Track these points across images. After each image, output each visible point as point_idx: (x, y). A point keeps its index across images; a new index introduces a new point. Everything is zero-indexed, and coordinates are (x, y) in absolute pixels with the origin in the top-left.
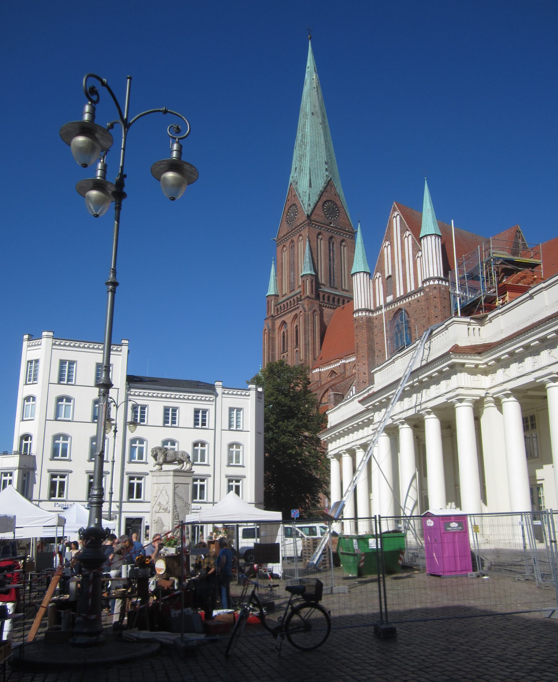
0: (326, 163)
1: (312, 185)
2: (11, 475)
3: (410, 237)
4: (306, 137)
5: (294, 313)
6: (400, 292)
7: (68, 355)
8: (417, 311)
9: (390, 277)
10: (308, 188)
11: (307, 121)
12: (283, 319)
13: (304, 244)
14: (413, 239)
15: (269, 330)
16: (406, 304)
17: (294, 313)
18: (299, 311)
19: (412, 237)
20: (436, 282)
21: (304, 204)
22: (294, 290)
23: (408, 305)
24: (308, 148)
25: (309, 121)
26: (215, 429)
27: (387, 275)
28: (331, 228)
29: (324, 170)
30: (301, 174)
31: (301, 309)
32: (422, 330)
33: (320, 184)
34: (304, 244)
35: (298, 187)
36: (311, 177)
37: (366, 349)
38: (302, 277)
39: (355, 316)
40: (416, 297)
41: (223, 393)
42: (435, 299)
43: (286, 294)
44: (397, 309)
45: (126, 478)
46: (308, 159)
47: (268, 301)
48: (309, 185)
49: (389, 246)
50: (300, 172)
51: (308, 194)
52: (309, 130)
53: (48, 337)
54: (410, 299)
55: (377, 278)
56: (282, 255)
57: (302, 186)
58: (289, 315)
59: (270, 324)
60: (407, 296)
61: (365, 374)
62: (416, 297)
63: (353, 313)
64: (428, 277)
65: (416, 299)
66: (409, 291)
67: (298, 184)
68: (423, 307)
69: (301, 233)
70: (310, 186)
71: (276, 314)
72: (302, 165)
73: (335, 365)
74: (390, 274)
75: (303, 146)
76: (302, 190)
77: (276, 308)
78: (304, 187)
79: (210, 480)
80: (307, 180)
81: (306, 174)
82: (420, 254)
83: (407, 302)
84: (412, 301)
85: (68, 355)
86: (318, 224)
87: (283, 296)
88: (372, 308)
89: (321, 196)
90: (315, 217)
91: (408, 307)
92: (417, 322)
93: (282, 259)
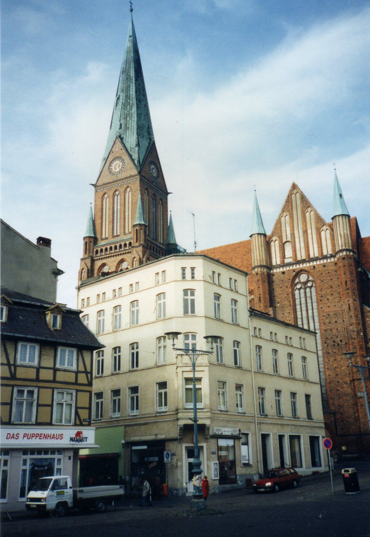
4: (131, 99)
5: (120, 258)
8: (324, 274)
11: (131, 84)
12: (104, 261)
15: (88, 270)
16: (310, 267)
17: (120, 258)
22: (118, 236)
23: (312, 268)
24: (134, 109)
27: (284, 240)
28: (153, 186)
31: (136, 255)
32: (330, 290)
33: (145, 143)
35: (124, 142)
37: (268, 300)
38: (134, 226)
39: (256, 270)
42: (351, 267)
43: (106, 238)
44: (300, 269)
46: (135, 118)
47: (86, 243)
49: (288, 217)
51: (137, 152)
56: (102, 201)
57: (129, 142)
58: (114, 258)
59: (89, 265)
63: (254, 268)
65: (322, 264)
67: (124, 139)
68: (330, 271)
69: (129, 185)
71: (95, 256)
72: (128, 123)
74: (289, 239)
75: (128, 107)
76: (129, 145)
77: (95, 250)
78: (132, 143)
81: (133, 133)
83: (311, 266)
84: (317, 265)
86: (146, 180)
87: (102, 239)
90: (144, 174)
92: (323, 283)
93: (102, 205)
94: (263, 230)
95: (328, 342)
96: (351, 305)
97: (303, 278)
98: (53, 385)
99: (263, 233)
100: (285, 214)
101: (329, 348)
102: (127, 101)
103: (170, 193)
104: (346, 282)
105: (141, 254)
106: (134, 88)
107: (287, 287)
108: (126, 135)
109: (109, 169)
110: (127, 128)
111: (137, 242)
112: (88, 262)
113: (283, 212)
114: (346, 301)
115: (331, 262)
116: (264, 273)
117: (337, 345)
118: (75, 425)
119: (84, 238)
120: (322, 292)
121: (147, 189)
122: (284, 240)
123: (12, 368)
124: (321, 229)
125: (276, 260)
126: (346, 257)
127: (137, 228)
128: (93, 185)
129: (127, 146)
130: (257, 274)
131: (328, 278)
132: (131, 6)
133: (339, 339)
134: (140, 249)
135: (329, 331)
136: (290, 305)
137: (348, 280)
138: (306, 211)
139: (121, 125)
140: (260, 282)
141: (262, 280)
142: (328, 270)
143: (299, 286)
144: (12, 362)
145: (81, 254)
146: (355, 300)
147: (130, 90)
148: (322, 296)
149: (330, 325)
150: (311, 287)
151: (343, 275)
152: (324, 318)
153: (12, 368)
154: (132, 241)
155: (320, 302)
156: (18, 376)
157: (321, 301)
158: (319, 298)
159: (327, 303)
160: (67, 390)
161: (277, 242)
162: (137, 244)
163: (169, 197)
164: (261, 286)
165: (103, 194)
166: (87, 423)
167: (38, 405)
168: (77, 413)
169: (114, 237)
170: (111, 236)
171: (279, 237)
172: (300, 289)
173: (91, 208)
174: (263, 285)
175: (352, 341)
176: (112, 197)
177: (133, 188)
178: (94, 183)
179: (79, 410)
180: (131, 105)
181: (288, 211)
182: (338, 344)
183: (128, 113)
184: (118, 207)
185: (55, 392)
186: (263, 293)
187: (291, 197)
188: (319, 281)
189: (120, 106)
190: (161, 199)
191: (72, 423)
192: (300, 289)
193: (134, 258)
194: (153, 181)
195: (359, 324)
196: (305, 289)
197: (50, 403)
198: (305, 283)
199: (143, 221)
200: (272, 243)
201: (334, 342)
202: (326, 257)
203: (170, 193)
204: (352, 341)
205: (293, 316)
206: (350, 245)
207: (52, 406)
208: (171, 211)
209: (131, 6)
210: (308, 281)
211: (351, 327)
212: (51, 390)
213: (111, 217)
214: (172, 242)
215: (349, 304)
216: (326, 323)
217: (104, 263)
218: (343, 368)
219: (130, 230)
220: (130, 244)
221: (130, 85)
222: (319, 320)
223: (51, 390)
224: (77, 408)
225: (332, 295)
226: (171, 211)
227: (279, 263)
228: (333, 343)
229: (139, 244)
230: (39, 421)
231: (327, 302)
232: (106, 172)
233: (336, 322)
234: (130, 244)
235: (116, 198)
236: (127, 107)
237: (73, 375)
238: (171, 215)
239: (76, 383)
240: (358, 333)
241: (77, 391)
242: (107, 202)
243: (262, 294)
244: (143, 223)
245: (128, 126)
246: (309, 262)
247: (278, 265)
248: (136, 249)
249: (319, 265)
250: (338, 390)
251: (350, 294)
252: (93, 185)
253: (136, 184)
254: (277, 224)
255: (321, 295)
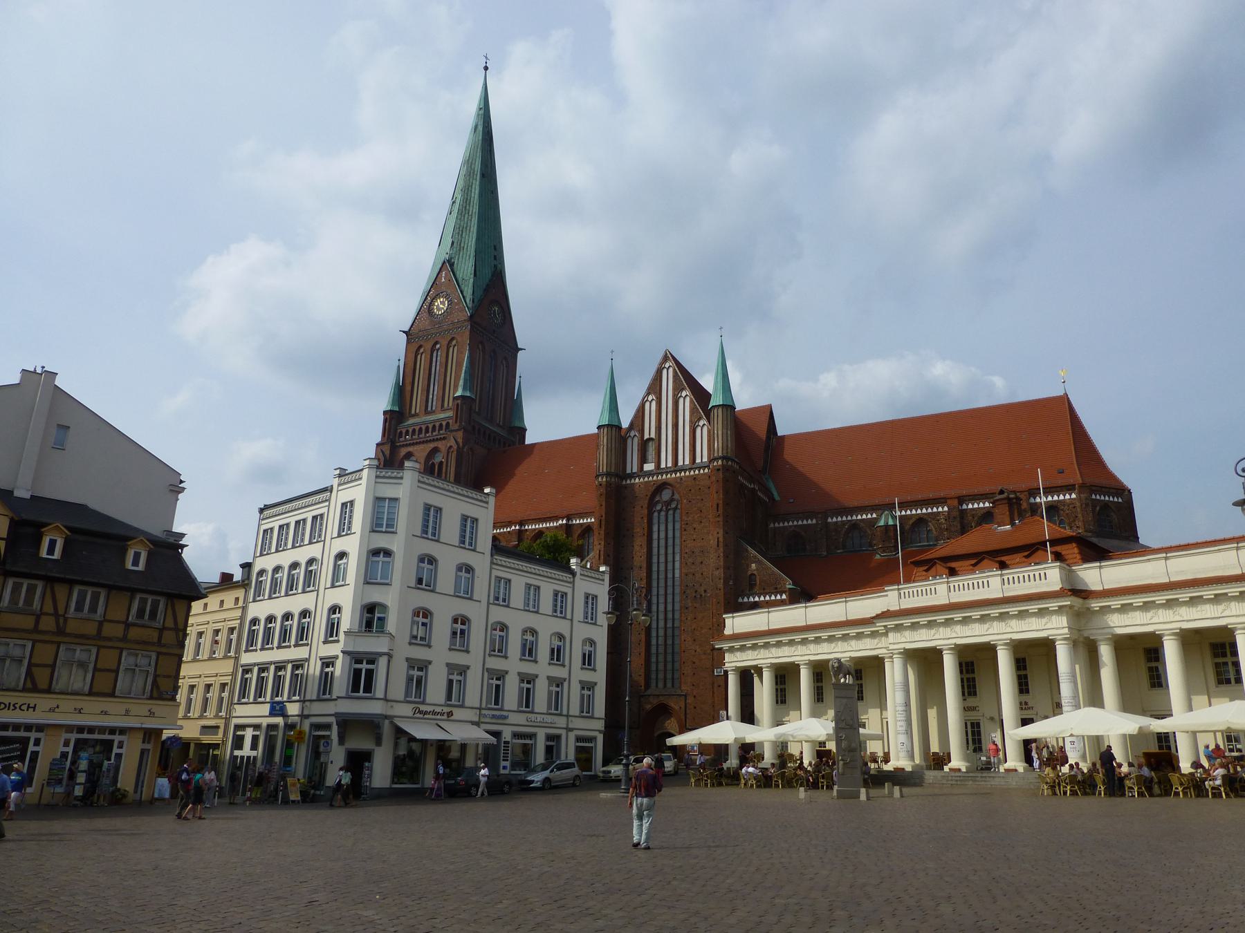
0: (495, 249)
1: (478, 273)
2: (371, 662)
3: (688, 399)
5: (432, 445)
6: (666, 461)
7: (436, 499)
8: (693, 491)
9: (650, 439)
10: (472, 276)
12: (410, 449)
13: (460, 352)
14: (691, 401)
16: (676, 478)
17: (432, 445)
18: (448, 445)
19: (691, 399)
20: (730, 463)
21: (464, 297)
22: (433, 412)
23: (679, 481)
24: (475, 221)
25: (478, 183)
26: (572, 620)
27: (646, 436)
29: (493, 259)
30: (461, 253)
31: (452, 442)
33: (487, 273)
34: (460, 352)
35: (455, 270)
36: (477, 263)
38: (455, 398)
40: (692, 473)
41: (581, 575)
45: (486, 674)
48: (473, 272)
49: (654, 403)
50: (460, 250)
52: (477, 196)
53: (413, 469)
54: (683, 474)
55: (630, 436)
58: (422, 446)
59: (387, 453)
60: (676, 468)
61: (608, 556)
62: (692, 473)
63: (597, 476)
64: (720, 454)
66: (680, 463)
70: (475, 275)
73: (502, 530)
74: (653, 436)
75: (466, 216)
76: (461, 274)
77: (399, 431)
79: (566, 684)
80: (470, 265)
82: (701, 423)
85: (436, 499)
88: (621, 473)
89: (487, 290)
91: (678, 483)
92: (690, 503)
94: (617, 420)
95: (688, 591)
96: (721, 540)
97: (666, 495)
98: (121, 645)
99: (616, 424)
100: (650, 398)
101: (689, 601)
102: (466, 207)
103: (522, 349)
104: (718, 505)
105: (460, 441)
106: (477, 188)
107: (642, 507)
108: (458, 259)
109: (430, 311)
110: (461, 249)
111: (456, 422)
112: (387, 449)
113: (648, 394)
114: (716, 532)
115: (704, 474)
116: (610, 484)
117: (699, 596)
118: (151, 698)
119: (385, 413)
120: (688, 517)
121: (481, 343)
122: (646, 436)
123: (61, 621)
124: (697, 424)
125: (632, 465)
126: (721, 468)
127: (459, 401)
128: (404, 332)
129: (457, 276)
130: (601, 485)
131: (698, 497)
132: (486, 63)
133: (703, 589)
134: (460, 435)
135: (691, 576)
136: (644, 535)
137: (721, 502)
138: (680, 395)
139: (453, 243)
140: (603, 498)
141: (606, 494)
142: (699, 485)
143: (658, 507)
144: (61, 612)
145: (378, 437)
146: (727, 533)
147: (471, 191)
148: (687, 524)
149: (693, 567)
150: (676, 508)
151: (715, 495)
152: (686, 555)
153: (61, 621)
154: (450, 421)
155: (683, 533)
156: (68, 630)
157: (685, 530)
158: (683, 526)
159: (693, 535)
160: (143, 652)
161: (636, 440)
162: (456, 427)
163: (520, 354)
164: (604, 504)
165: (417, 347)
166: (169, 697)
167: (95, 669)
168: (155, 683)
169: (427, 412)
170: (440, 409)
171: (639, 431)
172: (661, 510)
173: (399, 366)
174: (606, 502)
175: (717, 592)
176: (429, 353)
177: (459, 339)
178: (407, 330)
179: (158, 679)
180: (470, 213)
181: (655, 393)
182: (701, 595)
183: (465, 226)
184: (437, 367)
185: (124, 654)
186: (606, 514)
187: (661, 373)
188: (685, 501)
189: (455, 214)
190: (505, 358)
191: (146, 695)
192: (660, 511)
193: (451, 447)
194: (494, 331)
195: (729, 569)
196: (667, 511)
197: (114, 667)
198: (668, 503)
199: (468, 392)
200: (629, 441)
201: (696, 591)
202: (699, 468)
203: (522, 349)
204: (717, 592)
205: (645, 550)
206: (729, 450)
207: (117, 671)
208: (520, 377)
209: (486, 63)
210: (672, 500)
211: (717, 573)
212: (118, 651)
213: (426, 382)
214: (517, 424)
215: (718, 539)
216: (689, 564)
217: (409, 452)
218: (703, 631)
219: (450, 405)
220: (448, 424)
221: (472, 183)
222: (681, 558)
223: (118, 651)
224: (156, 676)
225: (701, 522)
226: (520, 377)
227: (635, 470)
228: (694, 594)
229: (459, 426)
230: (94, 690)
231: (692, 532)
232: (425, 315)
233: (702, 563)
234: (448, 424)
235: (435, 354)
236: (464, 216)
237: (156, 634)
238: (520, 382)
239: (159, 643)
240: (726, 583)
241: (159, 654)
242: (423, 361)
243: (604, 516)
244: (468, 394)
245: (462, 245)
246: (675, 472)
247: (634, 473)
248: (454, 433)
249: (688, 477)
250: (694, 663)
251: (721, 523)
252: (404, 332)
253: (464, 337)
254: (638, 411)
255: (685, 522)
